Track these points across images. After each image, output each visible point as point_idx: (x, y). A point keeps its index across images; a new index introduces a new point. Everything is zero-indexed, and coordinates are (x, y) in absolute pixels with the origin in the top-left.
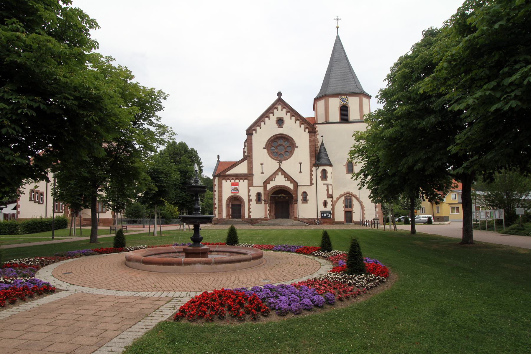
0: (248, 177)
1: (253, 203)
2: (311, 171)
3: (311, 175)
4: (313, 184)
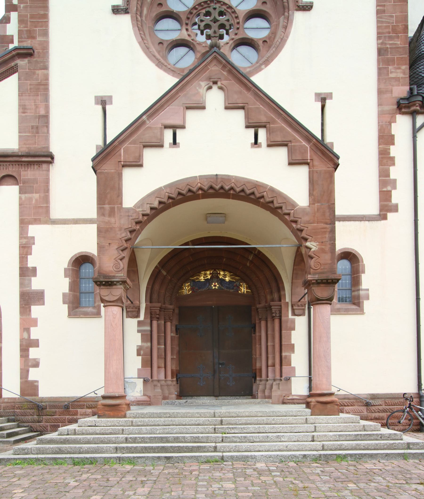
2: (386, 139)
3: (385, 160)
4: (395, 209)
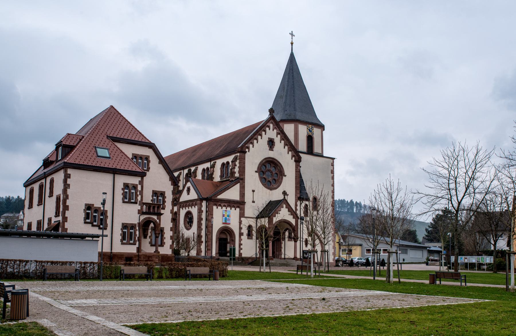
0: (240, 204)
1: (244, 237)
